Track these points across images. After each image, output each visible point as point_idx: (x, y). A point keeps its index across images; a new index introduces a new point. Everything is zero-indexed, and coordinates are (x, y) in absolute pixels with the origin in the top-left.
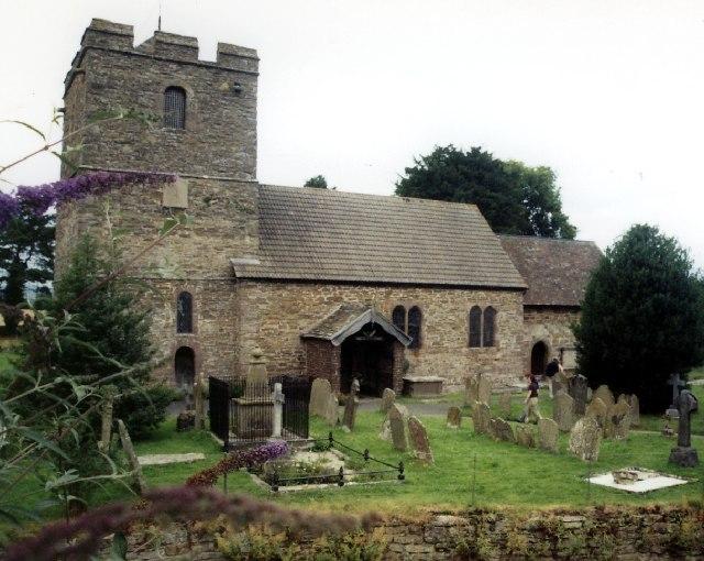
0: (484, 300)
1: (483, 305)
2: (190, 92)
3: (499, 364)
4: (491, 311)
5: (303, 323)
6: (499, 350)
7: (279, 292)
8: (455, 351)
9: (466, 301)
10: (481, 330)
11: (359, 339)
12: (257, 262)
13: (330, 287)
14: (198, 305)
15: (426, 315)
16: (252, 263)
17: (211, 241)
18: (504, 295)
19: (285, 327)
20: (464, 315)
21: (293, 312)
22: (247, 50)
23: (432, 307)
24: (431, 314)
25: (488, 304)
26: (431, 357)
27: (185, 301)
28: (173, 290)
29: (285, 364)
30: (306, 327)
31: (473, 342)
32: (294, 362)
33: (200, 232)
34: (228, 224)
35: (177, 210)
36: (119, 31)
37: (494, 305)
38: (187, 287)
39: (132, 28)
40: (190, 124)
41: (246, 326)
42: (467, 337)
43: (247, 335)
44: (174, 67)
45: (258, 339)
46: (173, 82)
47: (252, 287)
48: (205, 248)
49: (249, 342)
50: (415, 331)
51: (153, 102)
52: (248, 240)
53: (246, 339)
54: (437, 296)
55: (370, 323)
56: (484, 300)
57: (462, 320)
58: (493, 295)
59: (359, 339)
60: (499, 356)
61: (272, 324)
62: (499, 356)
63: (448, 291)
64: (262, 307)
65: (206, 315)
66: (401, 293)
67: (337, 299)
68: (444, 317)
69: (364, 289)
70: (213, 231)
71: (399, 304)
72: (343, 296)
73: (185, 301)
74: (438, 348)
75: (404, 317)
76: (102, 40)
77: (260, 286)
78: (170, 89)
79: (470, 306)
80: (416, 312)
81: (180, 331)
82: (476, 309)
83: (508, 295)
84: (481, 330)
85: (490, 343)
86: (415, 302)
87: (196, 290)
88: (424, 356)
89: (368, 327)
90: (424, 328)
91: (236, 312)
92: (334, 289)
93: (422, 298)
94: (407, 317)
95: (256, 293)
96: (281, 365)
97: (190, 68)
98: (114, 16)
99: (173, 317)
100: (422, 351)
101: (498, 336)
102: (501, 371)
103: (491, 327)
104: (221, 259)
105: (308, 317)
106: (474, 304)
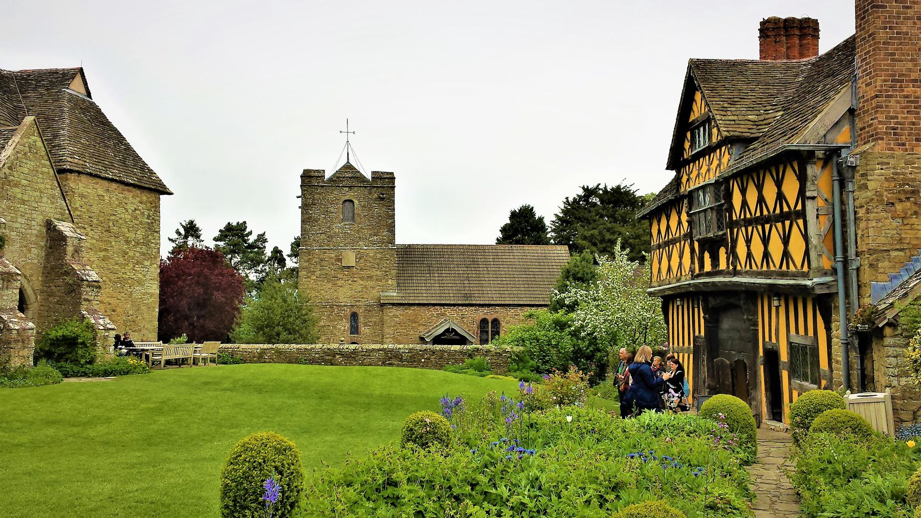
2: (356, 202)
5: (421, 328)
13: (438, 308)
14: (361, 319)
15: (503, 324)
16: (393, 295)
17: (371, 283)
21: (415, 322)
22: (387, 173)
23: (508, 318)
27: (354, 316)
28: (348, 312)
33: (362, 278)
35: (349, 267)
36: (317, 174)
38: (355, 310)
39: (324, 171)
40: (357, 219)
41: (386, 330)
44: (347, 189)
46: (347, 198)
48: (365, 287)
52: (390, 282)
54: (512, 311)
65: (366, 325)
66: (486, 310)
70: (370, 277)
73: (354, 316)
76: (310, 180)
78: (346, 201)
80: (496, 322)
81: (351, 333)
86: (495, 316)
87: (360, 312)
89: (447, 330)
91: (382, 322)
93: (499, 313)
95: (395, 311)
97: (356, 189)
98: (313, 166)
99: (348, 325)
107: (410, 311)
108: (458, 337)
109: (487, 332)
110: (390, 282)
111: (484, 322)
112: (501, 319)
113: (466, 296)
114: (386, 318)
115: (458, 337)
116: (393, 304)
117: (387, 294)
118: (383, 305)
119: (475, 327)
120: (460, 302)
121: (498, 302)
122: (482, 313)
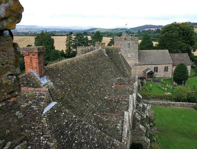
0: (166, 65)
4: (167, 67)
9: (164, 66)
10: (166, 69)
17: (133, 61)
18: (169, 65)
20: (164, 68)
30: (144, 70)
31: (165, 71)
50: (157, 70)
51: (127, 45)
54: (160, 65)
66: (155, 65)
68: (161, 68)
70: (133, 60)
74: (160, 72)
82: (165, 67)
83: (170, 65)
84: (166, 69)
85: (167, 71)
88: (158, 73)
90: (158, 70)
95: (138, 66)
101: (168, 70)
104: (134, 63)
107: (141, 66)
111: (155, 68)
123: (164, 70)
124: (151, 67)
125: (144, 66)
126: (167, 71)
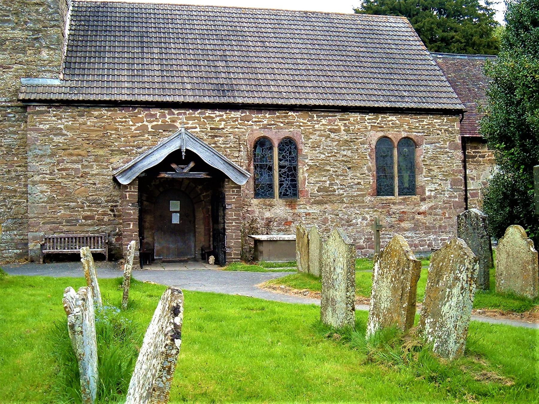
0: (397, 128)
1: (395, 135)
3: (427, 220)
6: (423, 200)
7: (81, 120)
8: (354, 200)
10: (395, 171)
11: (164, 175)
12: (57, 82)
13: (157, 112)
15: (305, 150)
18: (427, 120)
19: (92, 167)
21: (103, 146)
23: (314, 138)
24: (313, 148)
25: (404, 134)
26: (315, 210)
29: (91, 218)
31: (383, 188)
32: (104, 214)
34: (18, 33)
37: (413, 135)
41: (34, 164)
42: (372, 180)
43: (37, 178)
45: (51, 183)
47: (42, 113)
49: (39, 187)
50: (290, 173)
53: (34, 183)
54: (323, 122)
55: (179, 151)
56: (397, 128)
57: (362, 157)
58: (412, 120)
59: (164, 175)
60: (424, 207)
61: (73, 162)
62: (424, 207)
63: (339, 115)
64: (56, 139)
66: (266, 117)
67: (169, 128)
69: (208, 113)
71: (262, 133)
72: (177, 124)
74: (326, 196)
75: (272, 152)
77: (53, 111)
79: (374, 136)
80: (289, 146)
82: (384, 140)
84: (395, 171)
85: (410, 189)
86: (286, 132)
90: (303, 173)
92: (164, 116)
93: (296, 126)
94: (276, 150)
95: (51, 119)
96: (86, 218)
100: (302, 200)
101: (421, 179)
102: (428, 229)
103: (410, 167)
105: (125, 153)
106: (381, 134)
108: (203, 175)
109: (271, 169)
110: (45, 54)
111: (262, 143)
112: (301, 140)
113: (220, 89)
114: (32, 135)
115: (203, 175)
116: (49, 103)
117: (40, 81)
118: (26, 104)
119: (242, 158)
120: (206, 100)
121: (293, 102)
122: (257, 126)
123: (366, 174)
124: (215, 132)
125: (120, 114)
126: (410, 189)
